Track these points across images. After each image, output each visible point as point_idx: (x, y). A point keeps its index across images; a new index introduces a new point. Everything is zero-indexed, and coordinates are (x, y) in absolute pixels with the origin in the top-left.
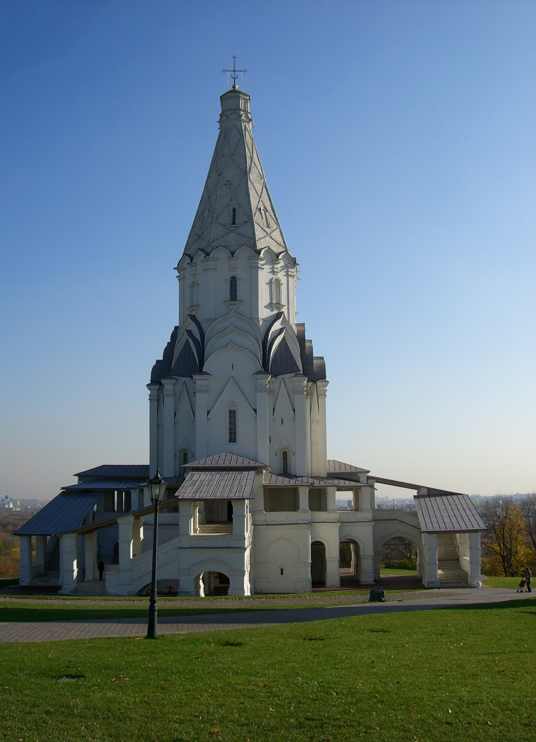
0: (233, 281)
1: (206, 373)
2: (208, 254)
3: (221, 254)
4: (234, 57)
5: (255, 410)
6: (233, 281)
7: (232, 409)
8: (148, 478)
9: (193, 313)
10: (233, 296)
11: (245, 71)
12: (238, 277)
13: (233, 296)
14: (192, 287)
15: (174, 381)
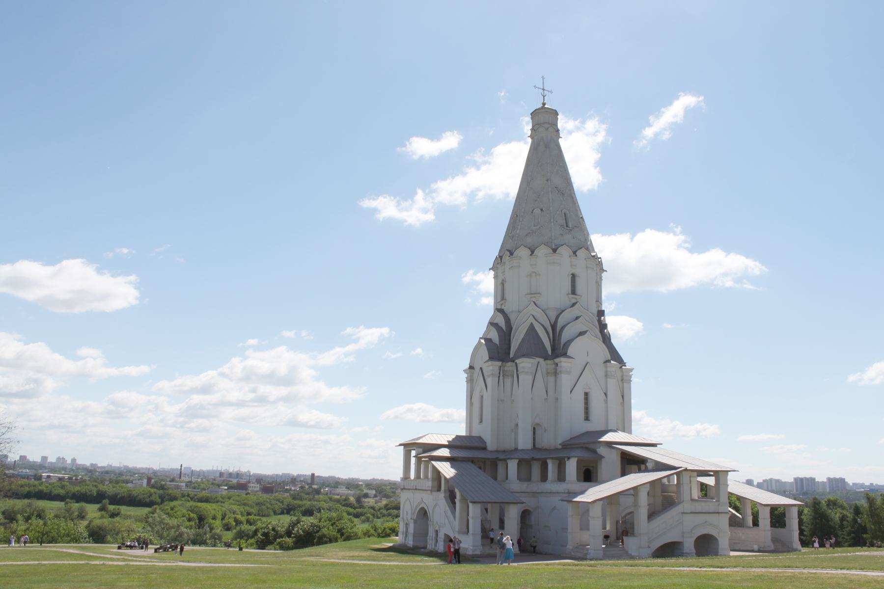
0: (574, 277)
1: (569, 357)
2: (555, 251)
3: (564, 251)
4: (543, 78)
5: (606, 394)
6: (574, 277)
7: (587, 391)
8: (485, 448)
9: (534, 300)
10: (574, 292)
11: (551, 92)
12: (577, 273)
13: (574, 292)
14: (530, 275)
15: (532, 360)
